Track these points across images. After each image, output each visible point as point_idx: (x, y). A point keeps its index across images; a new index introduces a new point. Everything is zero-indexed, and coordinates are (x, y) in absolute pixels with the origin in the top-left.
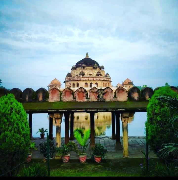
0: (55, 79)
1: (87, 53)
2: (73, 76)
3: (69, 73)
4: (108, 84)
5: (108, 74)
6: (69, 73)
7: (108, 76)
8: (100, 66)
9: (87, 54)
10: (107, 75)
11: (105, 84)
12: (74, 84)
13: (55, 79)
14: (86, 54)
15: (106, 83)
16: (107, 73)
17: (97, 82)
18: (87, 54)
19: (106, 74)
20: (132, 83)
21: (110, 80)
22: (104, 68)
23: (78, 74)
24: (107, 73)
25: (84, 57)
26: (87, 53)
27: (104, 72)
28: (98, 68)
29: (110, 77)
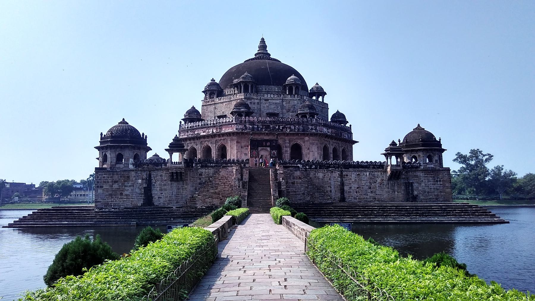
0: (124, 122)
1: (263, 41)
2: (210, 118)
3: (193, 107)
4: (344, 151)
5: (343, 116)
6: (193, 107)
7: (341, 122)
8: (310, 86)
9: (263, 45)
10: (340, 118)
11: (331, 151)
12: (208, 150)
13: (124, 122)
14: (258, 44)
15: (335, 150)
16: (338, 112)
17: (299, 142)
18: (263, 45)
19: (334, 116)
20: (439, 144)
21: (346, 136)
22: (323, 94)
23: (228, 113)
24: (338, 112)
25: (251, 52)
26: (263, 41)
27: (325, 107)
28: (301, 92)
29: (348, 125)
